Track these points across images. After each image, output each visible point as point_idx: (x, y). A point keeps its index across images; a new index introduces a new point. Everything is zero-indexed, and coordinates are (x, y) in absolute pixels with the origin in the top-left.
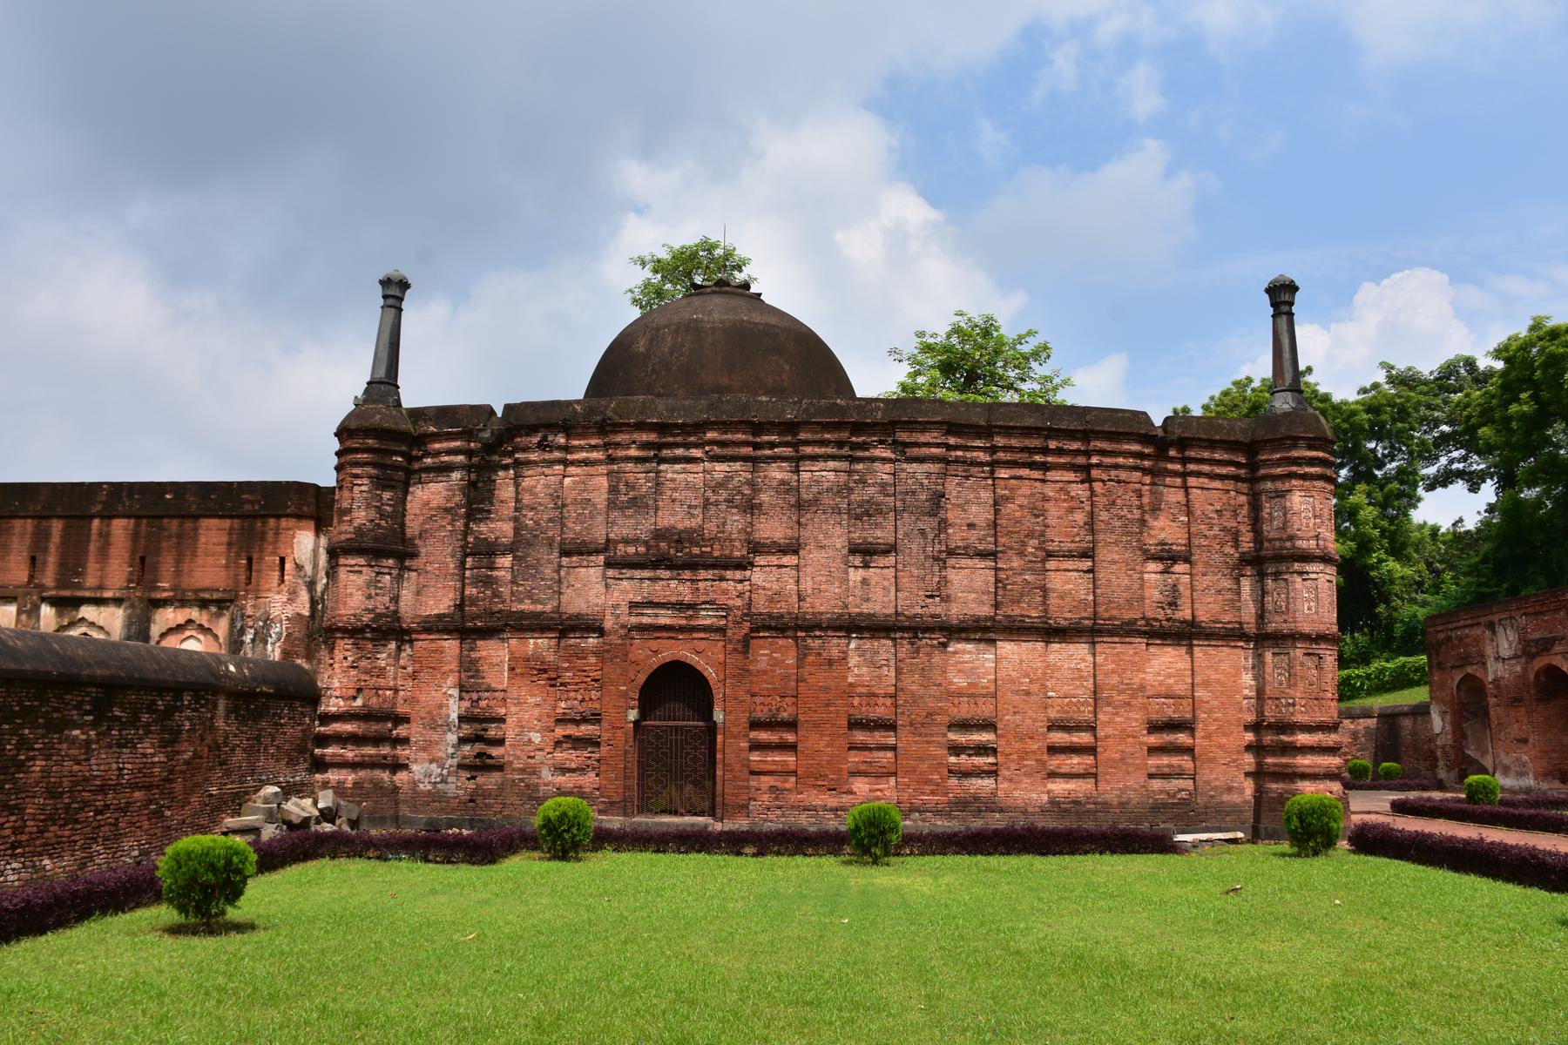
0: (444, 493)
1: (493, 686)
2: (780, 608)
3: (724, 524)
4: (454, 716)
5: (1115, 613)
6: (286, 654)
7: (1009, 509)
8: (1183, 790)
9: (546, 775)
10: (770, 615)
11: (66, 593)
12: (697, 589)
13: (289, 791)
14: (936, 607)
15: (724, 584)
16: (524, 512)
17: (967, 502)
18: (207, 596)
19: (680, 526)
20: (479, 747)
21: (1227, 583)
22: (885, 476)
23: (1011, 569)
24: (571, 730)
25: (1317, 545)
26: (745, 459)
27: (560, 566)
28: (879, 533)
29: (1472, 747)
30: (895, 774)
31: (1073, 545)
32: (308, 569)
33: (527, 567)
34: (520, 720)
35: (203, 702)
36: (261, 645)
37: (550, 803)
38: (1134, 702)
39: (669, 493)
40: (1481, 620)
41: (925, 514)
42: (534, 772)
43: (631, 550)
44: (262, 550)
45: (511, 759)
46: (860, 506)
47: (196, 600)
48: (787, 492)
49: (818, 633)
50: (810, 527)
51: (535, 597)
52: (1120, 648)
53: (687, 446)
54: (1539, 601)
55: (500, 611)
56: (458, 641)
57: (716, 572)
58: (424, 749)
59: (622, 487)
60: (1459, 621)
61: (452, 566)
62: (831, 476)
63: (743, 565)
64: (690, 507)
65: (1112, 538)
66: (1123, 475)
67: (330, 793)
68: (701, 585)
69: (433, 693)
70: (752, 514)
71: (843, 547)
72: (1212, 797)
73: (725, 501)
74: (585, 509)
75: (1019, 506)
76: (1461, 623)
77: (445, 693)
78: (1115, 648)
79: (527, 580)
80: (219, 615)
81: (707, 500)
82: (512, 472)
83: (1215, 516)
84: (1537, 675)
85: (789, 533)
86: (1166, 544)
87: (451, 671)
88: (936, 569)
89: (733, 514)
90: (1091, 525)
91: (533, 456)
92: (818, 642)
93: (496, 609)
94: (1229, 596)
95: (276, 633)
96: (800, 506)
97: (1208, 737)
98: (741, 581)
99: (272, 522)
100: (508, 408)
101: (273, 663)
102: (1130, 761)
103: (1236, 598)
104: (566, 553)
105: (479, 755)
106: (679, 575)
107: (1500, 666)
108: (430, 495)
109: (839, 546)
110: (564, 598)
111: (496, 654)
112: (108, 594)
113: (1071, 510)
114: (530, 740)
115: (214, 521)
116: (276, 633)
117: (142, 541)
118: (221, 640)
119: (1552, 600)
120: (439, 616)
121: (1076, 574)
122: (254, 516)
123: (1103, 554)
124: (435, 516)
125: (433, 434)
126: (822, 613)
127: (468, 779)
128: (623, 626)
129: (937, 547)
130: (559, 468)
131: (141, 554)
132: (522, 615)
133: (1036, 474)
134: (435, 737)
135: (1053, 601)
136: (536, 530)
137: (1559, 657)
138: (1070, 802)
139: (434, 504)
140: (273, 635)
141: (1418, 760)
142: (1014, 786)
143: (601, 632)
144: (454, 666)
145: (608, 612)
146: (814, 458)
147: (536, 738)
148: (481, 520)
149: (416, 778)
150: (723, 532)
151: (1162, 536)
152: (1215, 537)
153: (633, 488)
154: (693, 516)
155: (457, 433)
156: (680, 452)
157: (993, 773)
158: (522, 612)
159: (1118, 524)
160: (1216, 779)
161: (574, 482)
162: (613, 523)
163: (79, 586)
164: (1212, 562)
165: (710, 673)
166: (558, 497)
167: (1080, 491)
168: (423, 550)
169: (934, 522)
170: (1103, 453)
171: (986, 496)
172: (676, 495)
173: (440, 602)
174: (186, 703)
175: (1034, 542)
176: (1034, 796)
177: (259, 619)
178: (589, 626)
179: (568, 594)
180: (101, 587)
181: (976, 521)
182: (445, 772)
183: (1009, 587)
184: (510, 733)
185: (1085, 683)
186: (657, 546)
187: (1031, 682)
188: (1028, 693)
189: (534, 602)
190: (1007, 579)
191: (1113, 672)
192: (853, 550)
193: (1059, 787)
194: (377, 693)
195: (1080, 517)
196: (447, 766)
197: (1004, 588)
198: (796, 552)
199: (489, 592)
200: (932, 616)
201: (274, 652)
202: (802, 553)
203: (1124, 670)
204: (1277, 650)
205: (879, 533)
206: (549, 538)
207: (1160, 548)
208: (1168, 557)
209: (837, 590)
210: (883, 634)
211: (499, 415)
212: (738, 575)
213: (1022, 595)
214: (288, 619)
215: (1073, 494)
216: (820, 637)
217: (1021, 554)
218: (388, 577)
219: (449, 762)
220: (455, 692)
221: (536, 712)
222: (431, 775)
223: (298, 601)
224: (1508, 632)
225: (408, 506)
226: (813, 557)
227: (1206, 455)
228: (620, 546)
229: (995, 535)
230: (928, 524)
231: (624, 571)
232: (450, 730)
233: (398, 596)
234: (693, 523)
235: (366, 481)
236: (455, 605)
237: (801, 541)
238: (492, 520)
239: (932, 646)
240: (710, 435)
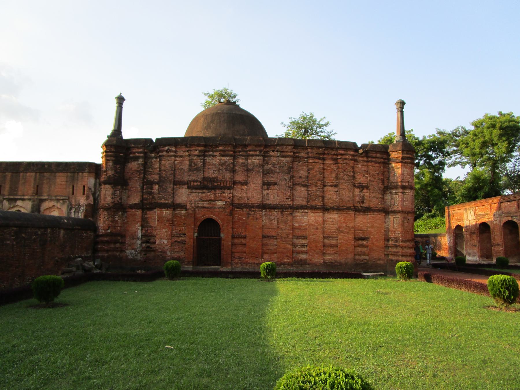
0: (136, 166)
1: (152, 226)
2: (242, 202)
3: (224, 176)
4: (140, 235)
5: (344, 204)
6: (86, 216)
7: (312, 172)
8: (365, 259)
9: (169, 253)
10: (238, 204)
11: (12, 197)
12: (216, 196)
13: (85, 259)
14: (290, 202)
15: (224, 195)
16: (162, 172)
17: (299, 170)
18: (59, 198)
19: (211, 177)
20: (148, 245)
21: (380, 196)
22: (274, 162)
23: (312, 191)
24: (176, 239)
25: (409, 184)
26: (231, 156)
27: (173, 189)
28: (272, 179)
30: (276, 253)
31: (332, 183)
32: (93, 189)
33: (163, 189)
34: (160, 236)
35: (55, 232)
36: (77, 213)
37: (168, 262)
38: (350, 232)
39: (207, 166)
40: (463, 208)
41: (286, 174)
42: (165, 252)
43: (196, 184)
44: (77, 184)
45: (158, 248)
46: (266, 171)
47: (56, 199)
48: (244, 166)
49: (253, 210)
50: (251, 177)
51: (166, 198)
52: (346, 215)
53: (212, 151)
55: (155, 202)
56: (141, 212)
57: (222, 191)
58: (130, 246)
59: (193, 165)
60: (456, 208)
61: (139, 188)
62: (257, 161)
63: (229, 188)
64: (214, 171)
65: (344, 181)
66: (348, 162)
67: (99, 260)
68: (217, 195)
69: (133, 228)
70: (233, 173)
71: (261, 183)
72: (374, 262)
73: (225, 169)
74: (181, 171)
75: (315, 171)
77: (137, 228)
78: (344, 215)
79: (163, 193)
80: (63, 204)
81: (219, 168)
82: (158, 159)
83: (376, 175)
85: (244, 179)
86: (361, 183)
87: (139, 221)
88: (289, 190)
89: (227, 173)
90: (337, 178)
91: (165, 154)
92: (253, 213)
93: (153, 202)
94: (380, 200)
95: (82, 210)
96: (248, 171)
97: (373, 243)
98: (229, 194)
99: (80, 174)
100: (157, 140)
101: (81, 220)
102: (348, 250)
103: (382, 200)
104: (176, 185)
105: (148, 247)
106: (210, 191)
108: (133, 165)
109: (260, 183)
110: (175, 199)
111: (154, 215)
112: (26, 197)
113: (332, 172)
114: (163, 243)
115: (61, 174)
116: (82, 210)
117: (38, 180)
118: (64, 212)
120: (135, 204)
121: (332, 192)
122: (74, 172)
123: (341, 186)
124: (134, 173)
125: (133, 147)
126: (254, 204)
127: (144, 255)
128: (193, 207)
129: (290, 184)
130: (173, 158)
131: (37, 185)
132: (161, 203)
133: (321, 161)
134: (134, 242)
135: (326, 201)
136: (166, 177)
138: (330, 263)
139: (133, 169)
140: (81, 210)
142: (312, 257)
143: (187, 209)
144: (140, 220)
145: (188, 203)
146: (252, 156)
147: (166, 242)
148: (148, 174)
149: (128, 254)
150: (224, 178)
151: (360, 181)
152: (376, 181)
153: (196, 165)
154: (215, 173)
155: (141, 147)
156: (211, 153)
157: (306, 253)
158: (161, 203)
159: (346, 177)
160: (375, 256)
161: (178, 163)
162: (190, 175)
163: (16, 195)
164: (375, 189)
165: (220, 222)
166: (173, 167)
167: (334, 167)
168: (130, 184)
169: (289, 176)
170: (341, 154)
171: (305, 168)
172: (209, 167)
173: (135, 200)
174: (49, 232)
175: (320, 182)
176: (319, 260)
177: (76, 205)
178: (183, 206)
179: (176, 197)
180: (24, 195)
181: (302, 176)
182: (137, 253)
183: (312, 196)
184: (158, 241)
185: (335, 226)
186: (204, 183)
187: (318, 225)
188: (317, 229)
189: (165, 200)
190: (311, 193)
191: (344, 222)
192: (264, 184)
193: (327, 258)
194: (115, 228)
195: (334, 175)
196: (137, 251)
197: (310, 196)
198: (246, 185)
199: (151, 197)
200: (288, 205)
201: (81, 216)
202: (248, 185)
203: (347, 222)
204: (395, 217)
205: (272, 179)
206: (169, 180)
207: (359, 184)
208: (361, 187)
209: (259, 197)
210: (273, 210)
211: (154, 141)
212: (229, 191)
213: (316, 198)
214: (86, 205)
215: (332, 167)
216: (254, 211)
217: (316, 186)
218: (118, 192)
219: (138, 249)
220: (140, 228)
221: (166, 234)
222: (132, 254)
223: (89, 199)
225: (125, 170)
226: (252, 186)
227: (374, 155)
228: (192, 183)
229: (308, 180)
230: (287, 177)
231: (193, 190)
232: (138, 240)
233: (122, 198)
234: (214, 176)
235: (111, 162)
236: (140, 201)
237: (248, 181)
238: (152, 174)
239: (288, 214)
240: (221, 148)
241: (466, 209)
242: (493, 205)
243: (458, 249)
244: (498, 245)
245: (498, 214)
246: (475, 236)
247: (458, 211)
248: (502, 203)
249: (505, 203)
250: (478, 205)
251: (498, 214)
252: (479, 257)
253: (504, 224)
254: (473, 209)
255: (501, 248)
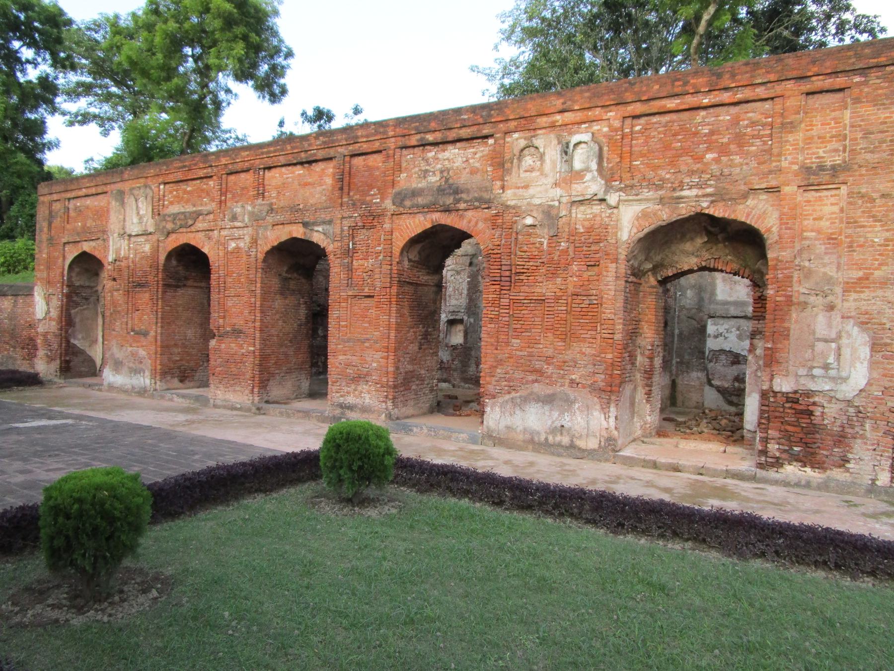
29: (80, 336)
40: (108, 188)
54: (185, 166)
60: (80, 189)
76: (84, 192)
84: (169, 256)
107: (124, 244)
119: (202, 166)
137: (201, 235)
141: (14, 347)
224: (140, 205)
241: (121, 193)
242: (232, 178)
243: (76, 342)
244: (237, 332)
245: (252, 214)
246: (144, 297)
247: (88, 202)
248: (269, 168)
249: (284, 169)
250: (171, 178)
251: (252, 214)
252: (153, 376)
253: (268, 253)
254: (148, 190)
255: (249, 345)
